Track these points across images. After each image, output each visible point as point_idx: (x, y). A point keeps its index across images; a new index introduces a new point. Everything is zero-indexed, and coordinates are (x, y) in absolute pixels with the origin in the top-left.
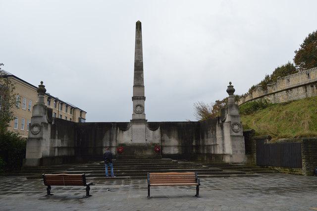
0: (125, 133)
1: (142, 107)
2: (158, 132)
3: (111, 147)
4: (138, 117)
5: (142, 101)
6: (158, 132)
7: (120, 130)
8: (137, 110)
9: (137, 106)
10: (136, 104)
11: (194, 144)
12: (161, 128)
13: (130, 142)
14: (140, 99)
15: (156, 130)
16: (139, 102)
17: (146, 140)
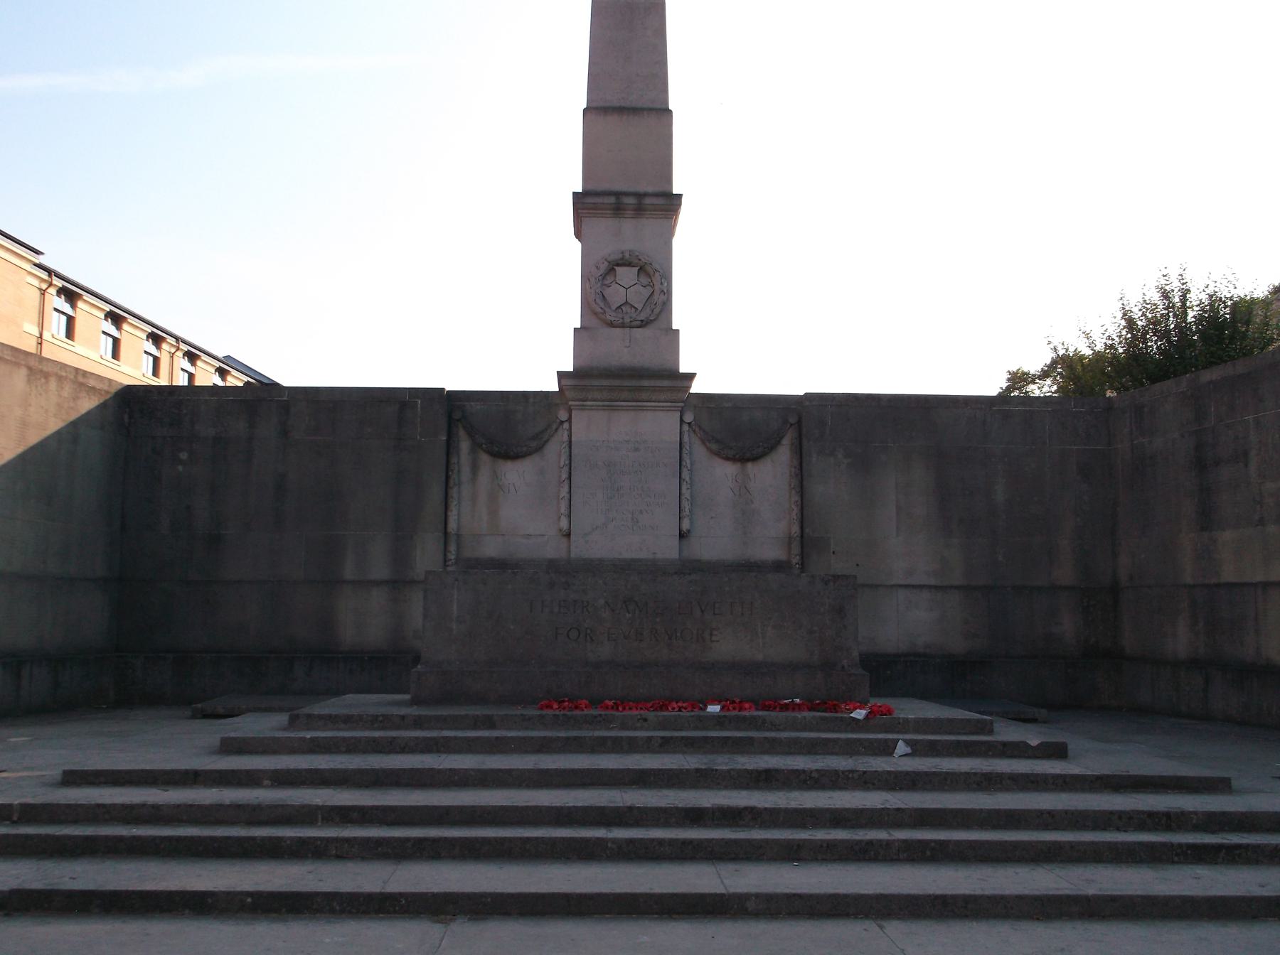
0: (517, 474)
1: (653, 275)
2: (772, 474)
3: (399, 583)
4: (621, 349)
5: (649, 225)
6: (772, 474)
7: (476, 446)
8: (616, 295)
9: (611, 270)
10: (611, 249)
11: (1065, 573)
12: (799, 452)
13: (552, 549)
14: (639, 210)
15: (755, 459)
16: (629, 235)
17: (682, 535)
